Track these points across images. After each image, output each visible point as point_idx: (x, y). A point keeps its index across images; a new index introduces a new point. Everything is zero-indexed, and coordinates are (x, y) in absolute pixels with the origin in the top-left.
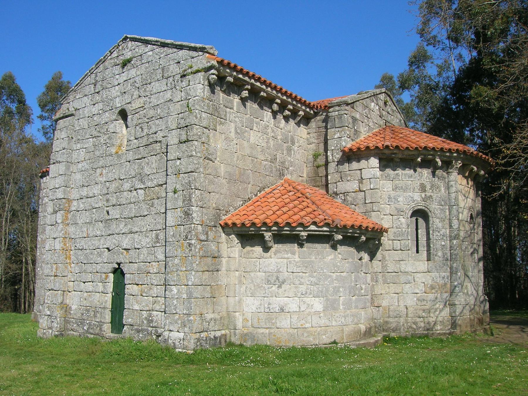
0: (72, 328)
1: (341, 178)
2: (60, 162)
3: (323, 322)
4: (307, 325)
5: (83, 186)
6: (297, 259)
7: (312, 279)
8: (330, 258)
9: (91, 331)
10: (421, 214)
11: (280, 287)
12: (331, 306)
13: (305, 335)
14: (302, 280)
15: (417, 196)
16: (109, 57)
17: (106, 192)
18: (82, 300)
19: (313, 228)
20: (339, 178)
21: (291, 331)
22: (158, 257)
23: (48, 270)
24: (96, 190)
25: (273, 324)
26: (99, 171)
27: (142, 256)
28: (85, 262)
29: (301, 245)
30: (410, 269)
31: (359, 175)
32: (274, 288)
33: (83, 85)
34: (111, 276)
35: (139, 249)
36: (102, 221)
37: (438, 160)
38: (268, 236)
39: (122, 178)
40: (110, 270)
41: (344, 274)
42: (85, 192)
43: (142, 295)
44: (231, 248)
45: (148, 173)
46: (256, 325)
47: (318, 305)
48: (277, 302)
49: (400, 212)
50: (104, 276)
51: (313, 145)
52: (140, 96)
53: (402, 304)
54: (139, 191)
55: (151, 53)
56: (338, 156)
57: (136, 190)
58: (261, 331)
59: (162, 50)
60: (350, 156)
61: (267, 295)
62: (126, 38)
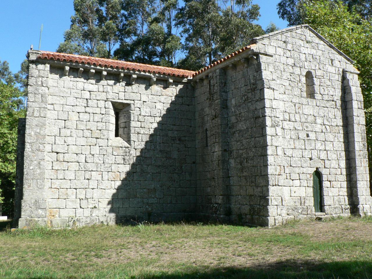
16: (295, 31)
17: (305, 121)
23: (272, 170)
28: (295, 166)
33: (275, 38)
35: (330, 160)
39: (315, 115)
57: (324, 125)
59: (330, 49)
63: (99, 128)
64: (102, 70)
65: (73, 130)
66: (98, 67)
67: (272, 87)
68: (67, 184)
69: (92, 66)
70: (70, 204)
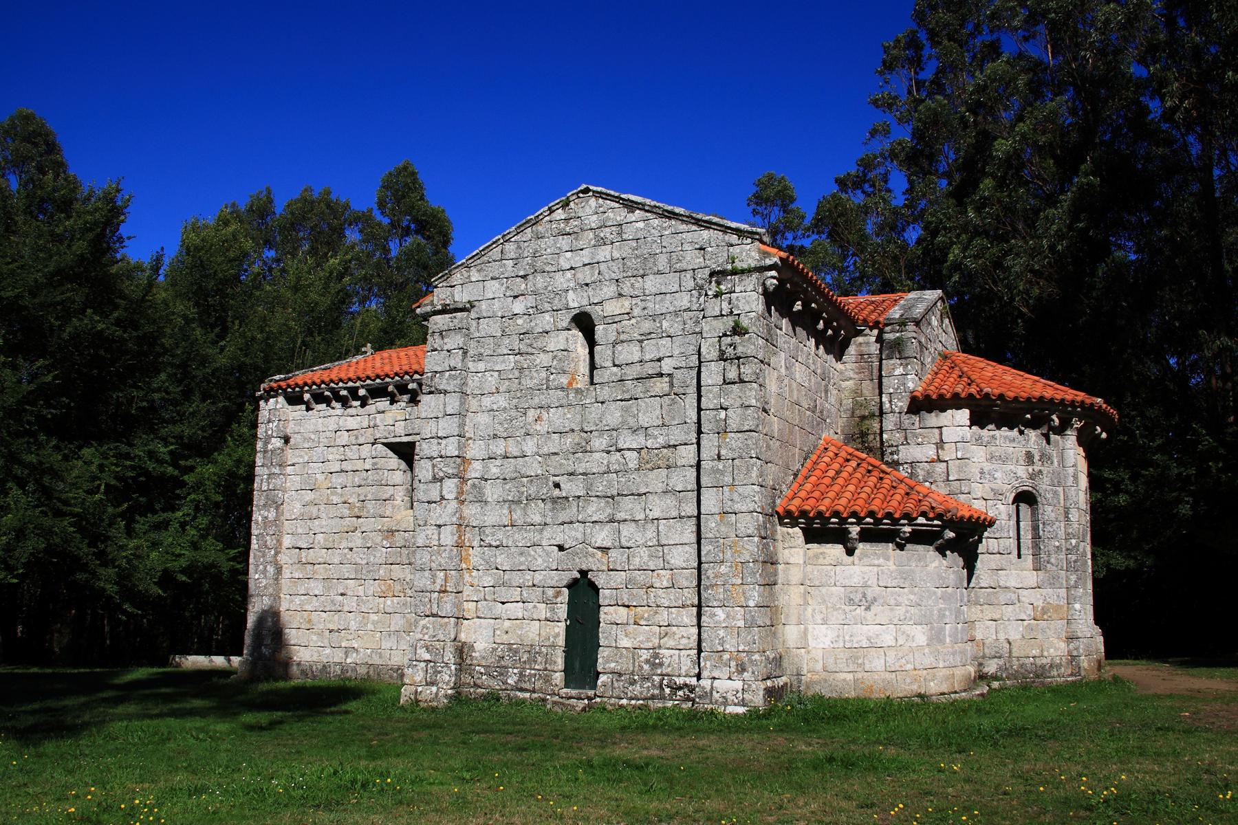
0: (478, 682)
1: (906, 439)
2: (446, 392)
3: (928, 661)
4: (909, 667)
5: (495, 436)
6: (893, 567)
7: (912, 597)
8: (933, 565)
9: (524, 686)
10: (1025, 498)
11: (868, 608)
12: (936, 638)
13: (908, 681)
14: (900, 599)
15: (1022, 471)
16: (548, 218)
18: (498, 632)
19: (921, 520)
20: (902, 439)
21: (888, 675)
22: (672, 561)
24: (530, 446)
25: (860, 665)
26: (532, 414)
27: (637, 559)
29: (901, 547)
30: (1012, 583)
31: (938, 437)
32: (858, 611)
33: (485, 258)
34: (566, 591)
36: (543, 500)
37: (1054, 417)
38: (855, 530)
40: (565, 582)
41: (950, 590)
42: (499, 447)
43: (636, 623)
44: (792, 546)
45: (646, 425)
46: (831, 667)
47: (920, 636)
48: (862, 634)
49: (998, 494)
50: (550, 592)
51: (851, 382)
52: (620, 295)
53: (1002, 637)
54: (628, 454)
55: (641, 225)
56: (902, 404)
58: (842, 676)
59: (667, 223)
60: (920, 405)
61: (847, 621)
62: (586, 191)
63: (362, 498)
64: (358, 388)
65: (322, 507)
66: (350, 384)
67: (441, 387)
68: (315, 603)
69: (341, 384)
70: (315, 638)
